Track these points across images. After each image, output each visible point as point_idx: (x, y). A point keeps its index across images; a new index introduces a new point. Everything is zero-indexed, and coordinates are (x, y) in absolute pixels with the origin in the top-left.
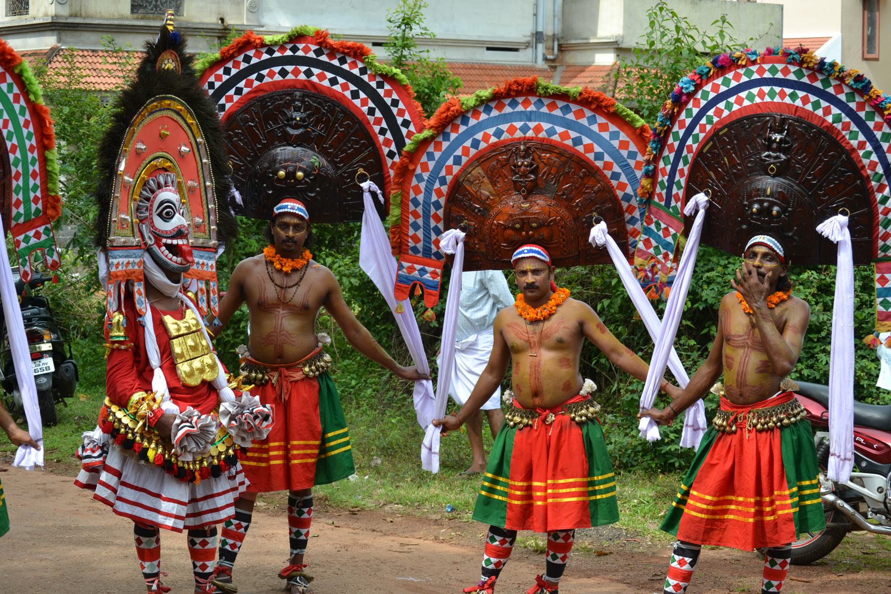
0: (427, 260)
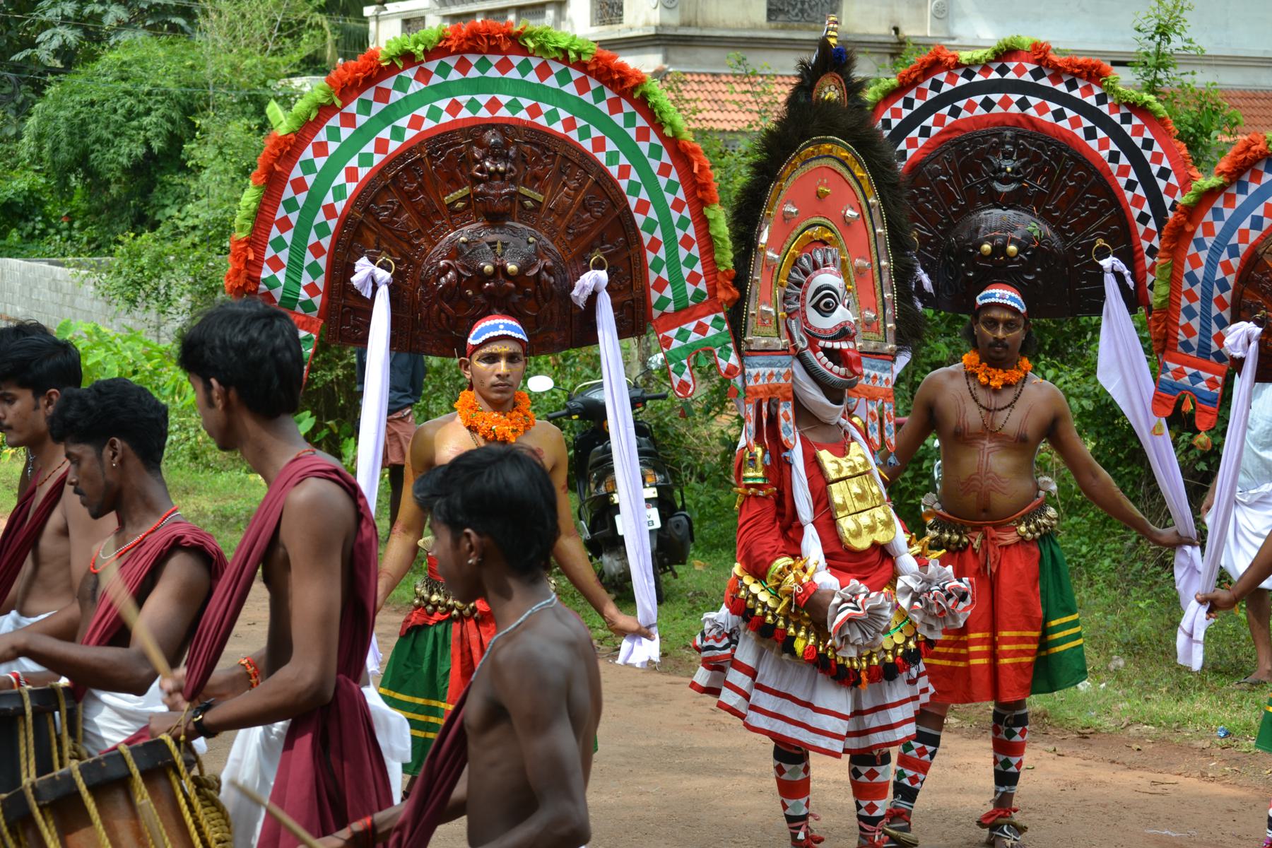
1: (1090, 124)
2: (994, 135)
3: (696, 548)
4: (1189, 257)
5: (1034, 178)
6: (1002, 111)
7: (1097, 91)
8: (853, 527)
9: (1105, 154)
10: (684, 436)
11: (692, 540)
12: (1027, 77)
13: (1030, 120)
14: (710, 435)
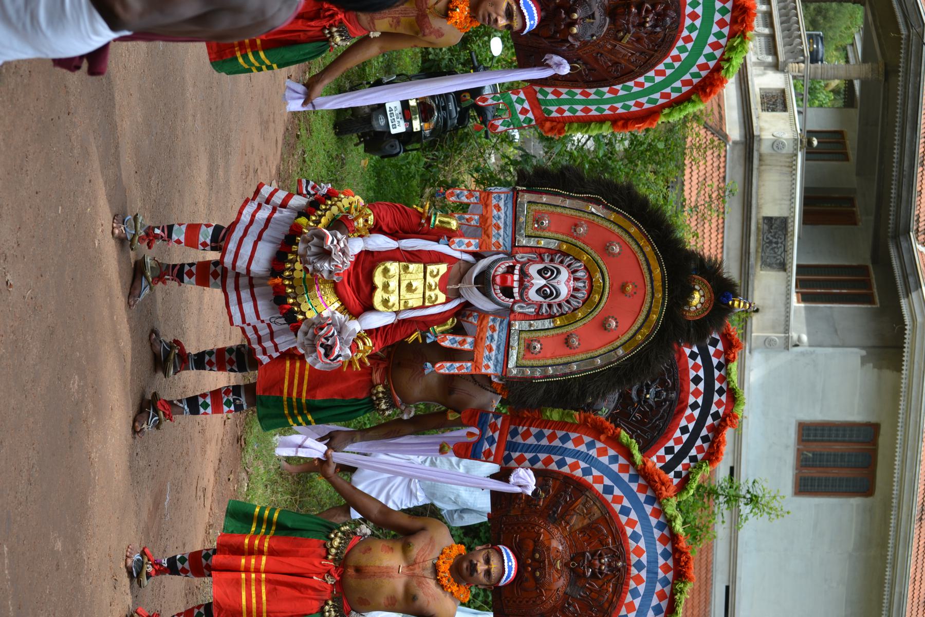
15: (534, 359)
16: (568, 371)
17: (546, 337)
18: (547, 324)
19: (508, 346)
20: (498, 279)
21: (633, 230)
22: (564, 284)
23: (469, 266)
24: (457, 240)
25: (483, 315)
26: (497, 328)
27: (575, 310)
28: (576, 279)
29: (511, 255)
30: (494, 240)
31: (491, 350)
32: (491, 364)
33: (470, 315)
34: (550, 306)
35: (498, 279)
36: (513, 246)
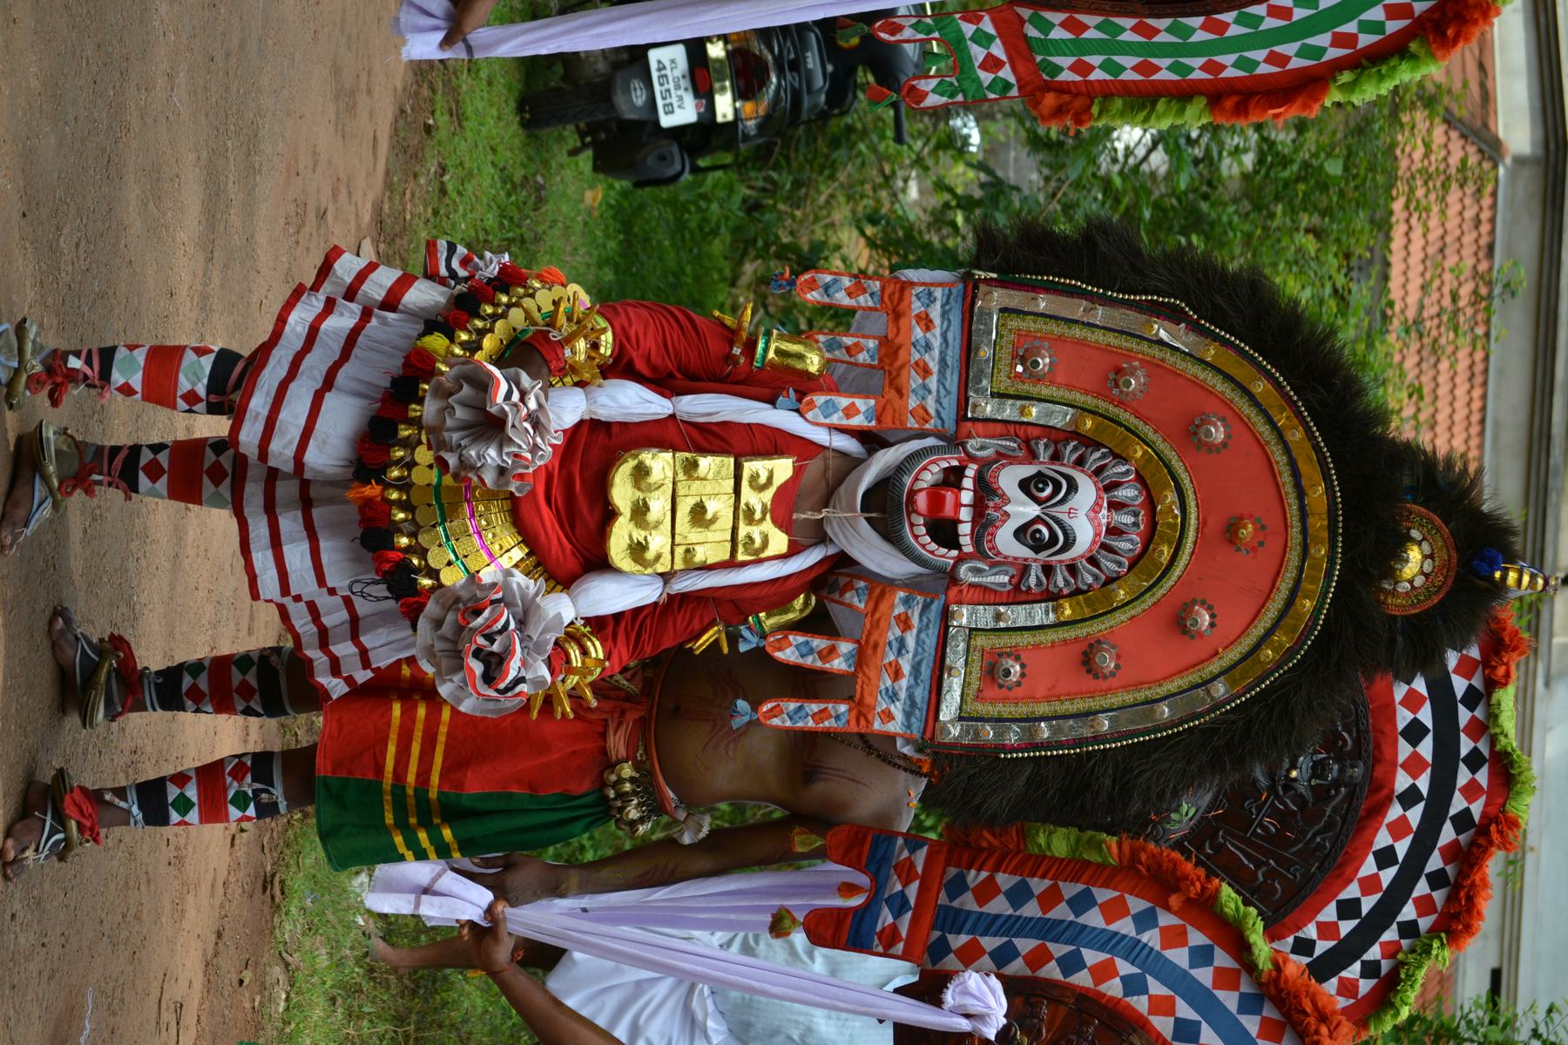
0: (926, 921)
1: (1365, 910)
2: (1357, 742)
3: (624, 194)
4: (1121, 899)
5: (1274, 814)
6: (1401, 759)
7: (1425, 923)
8: (655, 477)
9: (1311, 931)
10: (832, 177)
11: (639, 185)
12: (1458, 803)
13: (1381, 808)
14: (832, 225)
15: (1004, 700)
16: (1087, 732)
17: (1036, 646)
18: (1039, 614)
19: (940, 668)
20: (922, 501)
21: (1260, 387)
22: (1084, 518)
23: (851, 464)
24: (820, 399)
25: (880, 586)
26: (915, 621)
27: (1110, 581)
28: (1115, 506)
29: (954, 441)
30: (913, 402)
31: (897, 674)
32: (897, 710)
33: (849, 587)
34: (1048, 570)
35: (922, 501)
36: (961, 417)
